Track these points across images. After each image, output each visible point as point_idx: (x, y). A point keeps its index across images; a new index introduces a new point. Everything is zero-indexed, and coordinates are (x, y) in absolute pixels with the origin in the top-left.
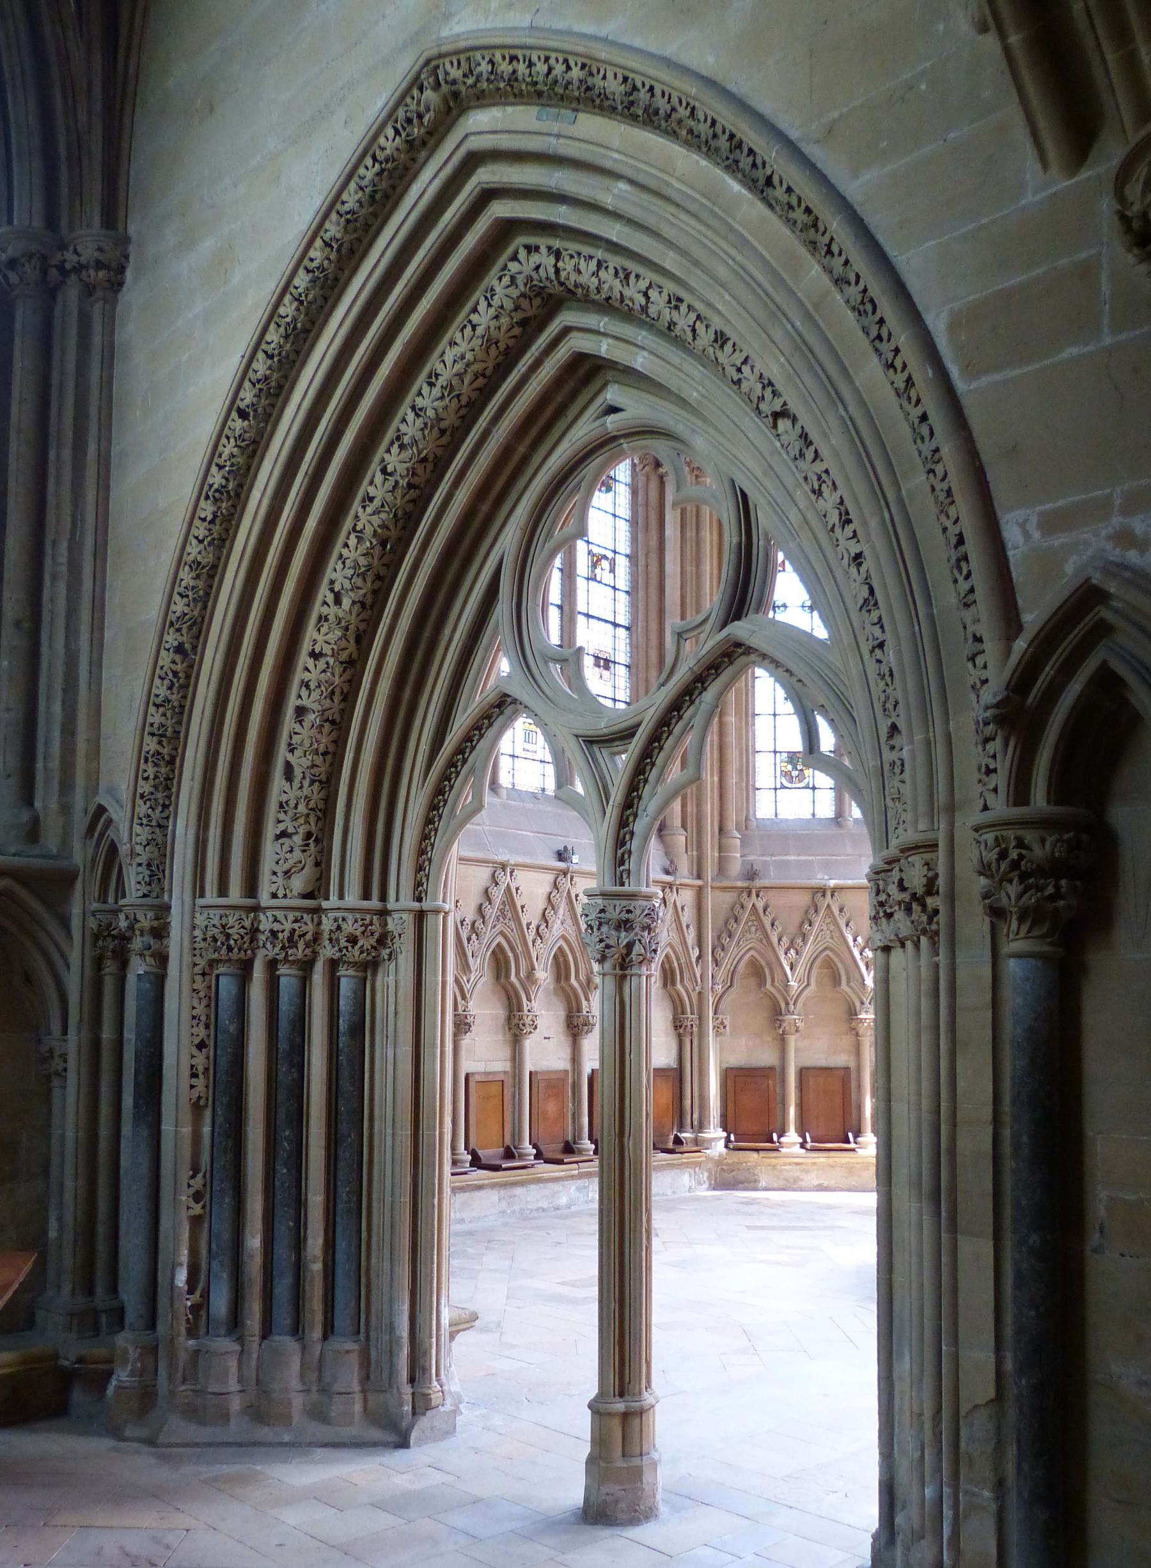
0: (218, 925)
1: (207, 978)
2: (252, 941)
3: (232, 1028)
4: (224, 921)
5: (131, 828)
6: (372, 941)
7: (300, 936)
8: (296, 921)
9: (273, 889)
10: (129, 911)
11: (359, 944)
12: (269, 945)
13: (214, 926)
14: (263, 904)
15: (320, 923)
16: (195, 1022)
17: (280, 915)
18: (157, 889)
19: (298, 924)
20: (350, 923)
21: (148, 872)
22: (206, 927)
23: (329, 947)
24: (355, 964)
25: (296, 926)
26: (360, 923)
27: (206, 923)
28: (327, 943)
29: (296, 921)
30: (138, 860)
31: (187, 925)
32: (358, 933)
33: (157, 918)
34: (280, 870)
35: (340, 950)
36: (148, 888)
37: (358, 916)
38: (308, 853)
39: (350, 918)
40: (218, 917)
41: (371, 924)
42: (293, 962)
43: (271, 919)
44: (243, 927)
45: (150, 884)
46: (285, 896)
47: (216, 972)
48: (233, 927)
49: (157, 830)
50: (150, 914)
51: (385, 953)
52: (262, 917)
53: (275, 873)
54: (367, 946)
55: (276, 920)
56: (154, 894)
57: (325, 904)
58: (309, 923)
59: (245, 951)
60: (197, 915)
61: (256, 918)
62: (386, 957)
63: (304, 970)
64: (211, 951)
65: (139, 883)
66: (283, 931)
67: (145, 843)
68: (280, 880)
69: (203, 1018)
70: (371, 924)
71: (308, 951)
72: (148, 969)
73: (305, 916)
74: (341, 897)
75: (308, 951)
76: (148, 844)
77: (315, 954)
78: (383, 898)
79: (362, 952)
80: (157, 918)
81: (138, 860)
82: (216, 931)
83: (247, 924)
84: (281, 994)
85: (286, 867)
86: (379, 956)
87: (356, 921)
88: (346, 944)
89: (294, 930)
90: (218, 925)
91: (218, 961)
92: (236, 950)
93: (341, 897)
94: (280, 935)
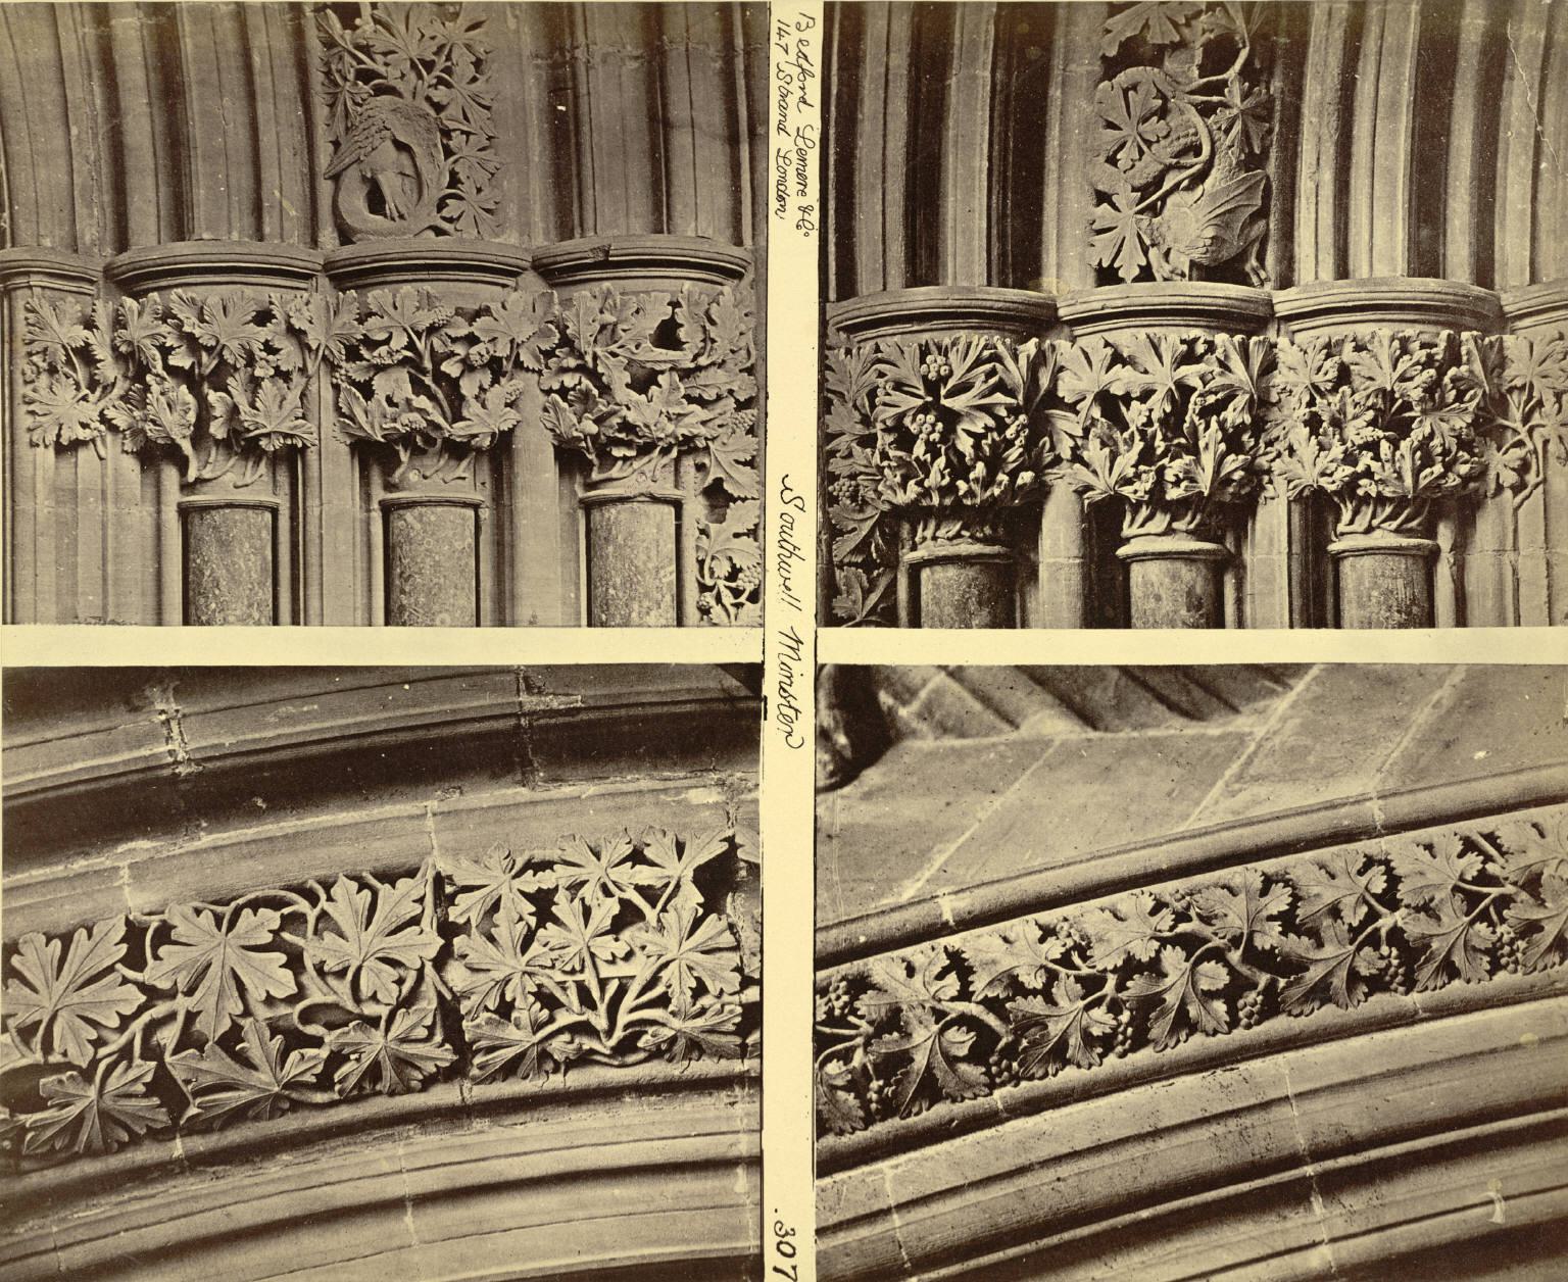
2: (1031, 444)
4: (934, 365)
6: (1460, 422)
7: (1206, 413)
8: (1189, 357)
11: (1417, 434)
12: (1095, 452)
15: (1269, 366)
17: (1129, 338)
19: (1201, 367)
23: (1307, 448)
24: (1401, 503)
25: (1191, 373)
26: (1421, 355)
37: (1410, 331)
40: (912, 351)
42: (1177, 509)
43: (1102, 355)
44: (1001, 387)
46: (1146, 274)
47: (908, 557)
48: (964, 388)
51: (1501, 464)
53: (1102, 198)
55: (1117, 359)
57: (1285, 302)
58: (1236, 363)
62: (1510, 478)
66: (1146, 395)
68: (1127, 217)
70: (1454, 356)
71: (1233, 463)
73: (1221, 338)
75: (1233, 463)
77: (1256, 476)
78: (1484, 272)
83: (1016, 373)
85: (1148, 169)
86: (1481, 474)
88: (1370, 434)
89: (1185, 390)
91: (915, 513)
93: (1343, 271)
94: (1135, 414)
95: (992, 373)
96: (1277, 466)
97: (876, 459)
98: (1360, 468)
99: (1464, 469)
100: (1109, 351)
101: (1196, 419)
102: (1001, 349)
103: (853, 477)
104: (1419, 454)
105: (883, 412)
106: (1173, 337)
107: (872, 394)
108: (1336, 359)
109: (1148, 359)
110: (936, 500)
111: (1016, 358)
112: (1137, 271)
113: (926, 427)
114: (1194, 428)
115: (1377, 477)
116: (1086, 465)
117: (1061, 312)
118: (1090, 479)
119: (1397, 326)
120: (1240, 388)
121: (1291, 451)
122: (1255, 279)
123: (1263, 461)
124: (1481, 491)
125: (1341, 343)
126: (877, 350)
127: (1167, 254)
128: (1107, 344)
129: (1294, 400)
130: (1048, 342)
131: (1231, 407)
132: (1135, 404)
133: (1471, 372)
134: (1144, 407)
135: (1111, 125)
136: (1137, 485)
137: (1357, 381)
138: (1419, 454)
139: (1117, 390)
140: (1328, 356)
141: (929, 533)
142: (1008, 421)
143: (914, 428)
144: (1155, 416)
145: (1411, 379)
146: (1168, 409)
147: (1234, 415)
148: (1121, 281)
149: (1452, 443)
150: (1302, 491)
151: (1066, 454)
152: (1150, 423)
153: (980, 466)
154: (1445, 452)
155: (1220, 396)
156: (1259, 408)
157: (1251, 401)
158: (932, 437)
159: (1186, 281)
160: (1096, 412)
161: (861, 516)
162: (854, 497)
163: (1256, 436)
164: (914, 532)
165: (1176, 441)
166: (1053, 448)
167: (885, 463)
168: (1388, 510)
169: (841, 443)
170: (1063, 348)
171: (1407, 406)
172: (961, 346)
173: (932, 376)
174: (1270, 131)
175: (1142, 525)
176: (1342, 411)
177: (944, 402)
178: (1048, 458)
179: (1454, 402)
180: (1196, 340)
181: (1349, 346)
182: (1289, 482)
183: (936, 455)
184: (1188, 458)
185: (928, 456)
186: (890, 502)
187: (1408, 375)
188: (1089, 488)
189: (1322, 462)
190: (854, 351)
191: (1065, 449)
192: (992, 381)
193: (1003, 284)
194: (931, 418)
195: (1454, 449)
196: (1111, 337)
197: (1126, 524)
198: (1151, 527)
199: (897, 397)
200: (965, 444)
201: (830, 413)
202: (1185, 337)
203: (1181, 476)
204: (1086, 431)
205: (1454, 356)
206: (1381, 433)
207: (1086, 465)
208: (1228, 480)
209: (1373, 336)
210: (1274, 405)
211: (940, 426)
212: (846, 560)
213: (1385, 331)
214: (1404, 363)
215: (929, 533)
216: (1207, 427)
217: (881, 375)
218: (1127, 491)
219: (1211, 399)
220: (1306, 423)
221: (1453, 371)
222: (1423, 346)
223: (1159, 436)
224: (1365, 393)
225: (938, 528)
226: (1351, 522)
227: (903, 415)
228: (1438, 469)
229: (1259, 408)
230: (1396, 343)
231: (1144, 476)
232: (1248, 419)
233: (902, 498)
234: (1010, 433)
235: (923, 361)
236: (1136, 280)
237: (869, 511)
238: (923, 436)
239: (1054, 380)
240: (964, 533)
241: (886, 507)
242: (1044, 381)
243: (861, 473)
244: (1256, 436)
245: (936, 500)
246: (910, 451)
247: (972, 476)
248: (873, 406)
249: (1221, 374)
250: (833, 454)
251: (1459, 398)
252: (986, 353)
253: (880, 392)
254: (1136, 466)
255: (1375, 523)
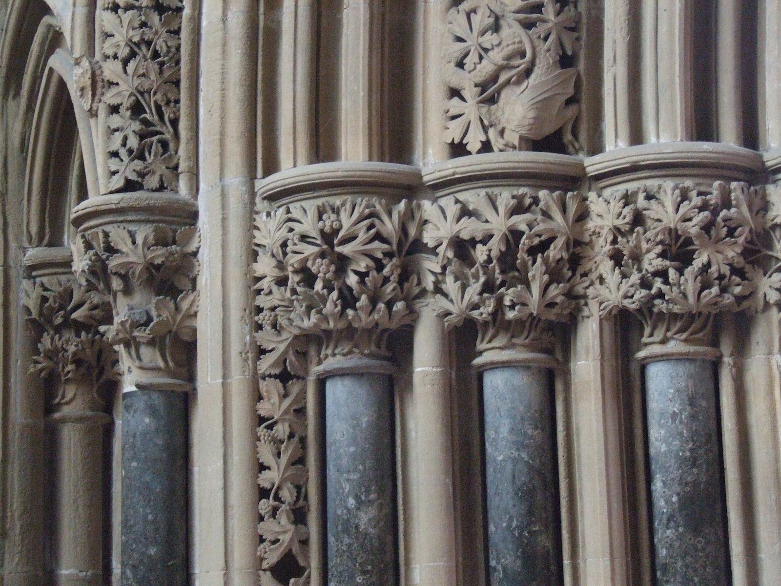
0: (314, 233)
1: (295, 388)
2: (404, 278)
3: (365, 518)
5: (91, 19)
6: (732, 253)
7: (533, 251)
8: (519, 209)
9: (454, 132)
10: (96, 228)
11: (699, 261)
12: (451, 285)
13: (304, 238)
14: (428, 178)
15: (583, 216)
16: (265, 506)
17: (474, 198)
18: (161, 169)
19: (528, 216)
20: (669, 199)
21: (136, 126)
22: (284, 245)
24: (691, 317)
25: (520, 221)
26: (697, 201)
27: (283, 233)
28: (606, 267)
29: (519, 209)
30: (110, 97)
31: (236, 250)
32: (693, 229)
33: (162, 241)
34: (467, 82)
35: (645, 284)
36: (138, 165)
37: (688, 183)
38: (541, 29)
39: (668, 188)
40: (312, 213)
41: (726, 203)
42: (513, 329)
43: (452, 210)
44: (378, 237)
45: (141, 157)
46: (486, 147)
47: (316, 370)
48: (350, 239)
49: (155, 19)
50: (143, 232)
52: (428, 208)
54: (719, 267)
55: (465, 212)
56: (152, 181)
59: (390, 304)
60: (261, 220)
61: (410, 214)
63: (549, 351)
64: (300, 309)
65: (115, 154)
67: (124, 52)
68: (470, 108)
69: (287, 494)
71: (555, 291)
72: (146, 378)
73: (542, 194)
74: (637, 137)
75: (555, 291)
76: (133, 55)
77: (575, 299)
79: (706, 285)
80: (162, 241)
81: (110, 97)
82: (309, 250)
83: (389, 226)
84: (490, 418)
85: (486, 68)
86: (750, 295)
87: (685, 196)
88: (659, 263)
90: (314, 233)
92: (364, 300)
94: (480, 253)
95: (371, 227)
96: (591, 292)
97: (288, 294)
98: (654, 291)
99: (737, 290)
100: (459, 206)
101: (525, 256)
102: (378, 207)
103: (273, 309)
104: (699, 278)
105: (292, 257)
106: (505, 197)
107: (284, 245)
108: (632, 206)
109: (488, 213)
110: (332, 324)
111: (390, 214)
112: (479, 146)
113: (320, 267)
114: (525, 263)
115: (667, 298)
116: (446, 295)
117: (425, 179)
118: (447, 305)
119: (678, 180)
120: (559, 232)
121: (602, 280)
122: (571, 149)
123: (580, 289)
124: (753, 309)
125: (635, 193)
126: (288, 211)
127: (502, 133)
128: (457, 201)
129: (601, 241)
130: (415, 202)
131: (552, 246)
132: (479, 247)
133: (740, 213)
134: (485, 248)
135: (460, 39)
136: (482, 310)
137: (649, 223)
138: (699, 278)
139: (465, 235)
140: (626, 205)
141: (329, 351)
142: (384, 262)
143: (314, 269)
144: (494, 254)
145: (690, 220)
146: (503, 249)
147: (554, 252)
148: (469, 153)
149: (726, 270)
150: (610, 312)
151: (430, 286)
152: (489, 260)
153: (364, 297)
154: (721, 277)
155: (543, 238)
156: (575, 246)
157: (567, 245)
158: (327, 276)
159: (517, 152)
160: (450, 254)
161: (280, 339)
162: (274, 326)
163: (573, 269)
164: (319, 353)
165: (511, 274)
166: (419, 283)
167: (294, 297)
168: (679, 325)
169: (265, 284)
170: (428, 208)
171: (689, 241)
172: (348, 206)
173: (327, 229)
174: (578, 39)
175: (490, 341)
176: (638, 246)
177: (338, 249)
178: (417, 290)
179: (727, 236)
180: (524, 196)
181: (641, 197)
182: (601, 304)
183: (330, 292)
184: (519, 287)
185: (325, 291)
186: (300, 328)
187: (688, 217)
188: (447, 314)
189: (624, 287)
190: (272, 214)
191: (429, 282)
192: (373, 231)
193: (382, 159)
194: (326, 261)
195: (728, 273)
196: (461, 196)
197: (478, 342)
198: (495, 343)
199: (301, 246)
200: (352, 280)
201: (256, 261)
202: (515, 193)
203: (514, 300)
204: (444, 268)
205: (726, 203)
206: (667, 263)
207: (446, 295)
208: (551, 305)
209: (660, 187)
210: (587, 244)
211: (333, 268)
212: (267, 373)
213: (669, 184)
214: (685, 207)
215: (329, 351)
216: (534, 262)
217: (291, 230)
218: (475, 314)
219: (536, 241)
220: (612, 257)
221: (724, 213)
222: (700, 194)
223: (497, 271)
224: (654, 232)
225: (336, 347)
226: (651, 335)
227: (306, 260)
228: (715, 290)
229: (575, 246)
230: (677, 192)
231: (487, 302)
232: (565, 256)
233: (307, 324)
234: (386, 271)
235: (320, 218)
236: (479, 152)
237: (285, 335)
238: (321, 275)
239: (420, 230)
240: (356, 350)
241: (296, 332)
242: (412, 231)
243: (279, 306)
244: (573, 269)
245: (332, 324)
246: (313, 288)
247: (358, 304)
248: (285, 254)
249: (543, 221)
250: (259, 292)
251: (731, 233)
252: (367, 211)
253: (289, 243)
254: (481, 294)
255: (669, 334)
